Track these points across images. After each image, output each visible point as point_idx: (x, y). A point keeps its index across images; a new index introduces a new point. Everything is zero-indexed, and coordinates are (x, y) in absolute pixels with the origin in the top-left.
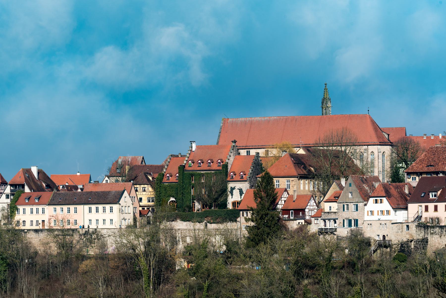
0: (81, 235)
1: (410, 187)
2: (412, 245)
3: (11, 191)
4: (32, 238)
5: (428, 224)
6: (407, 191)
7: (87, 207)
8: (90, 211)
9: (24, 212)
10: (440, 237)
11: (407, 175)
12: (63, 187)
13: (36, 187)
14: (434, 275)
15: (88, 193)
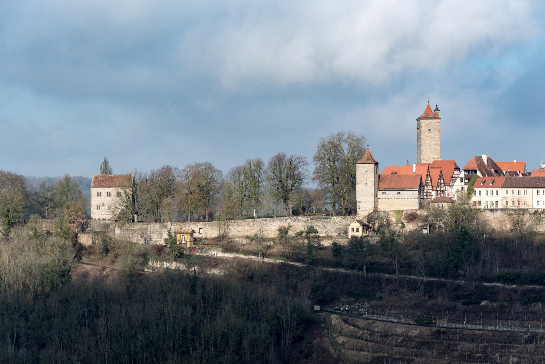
0: (531, 214)
3: (465, 175)
4: (488, 217)
7: (535, 190)
8: (538, 193)
9: (480, 194)
12: (506, 172)
13: (487, 173)
15: (536, 178)
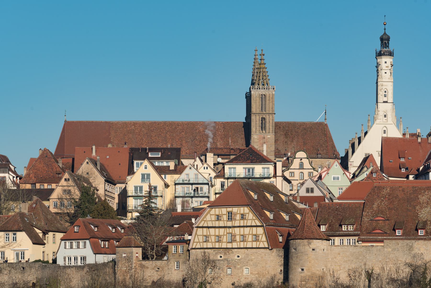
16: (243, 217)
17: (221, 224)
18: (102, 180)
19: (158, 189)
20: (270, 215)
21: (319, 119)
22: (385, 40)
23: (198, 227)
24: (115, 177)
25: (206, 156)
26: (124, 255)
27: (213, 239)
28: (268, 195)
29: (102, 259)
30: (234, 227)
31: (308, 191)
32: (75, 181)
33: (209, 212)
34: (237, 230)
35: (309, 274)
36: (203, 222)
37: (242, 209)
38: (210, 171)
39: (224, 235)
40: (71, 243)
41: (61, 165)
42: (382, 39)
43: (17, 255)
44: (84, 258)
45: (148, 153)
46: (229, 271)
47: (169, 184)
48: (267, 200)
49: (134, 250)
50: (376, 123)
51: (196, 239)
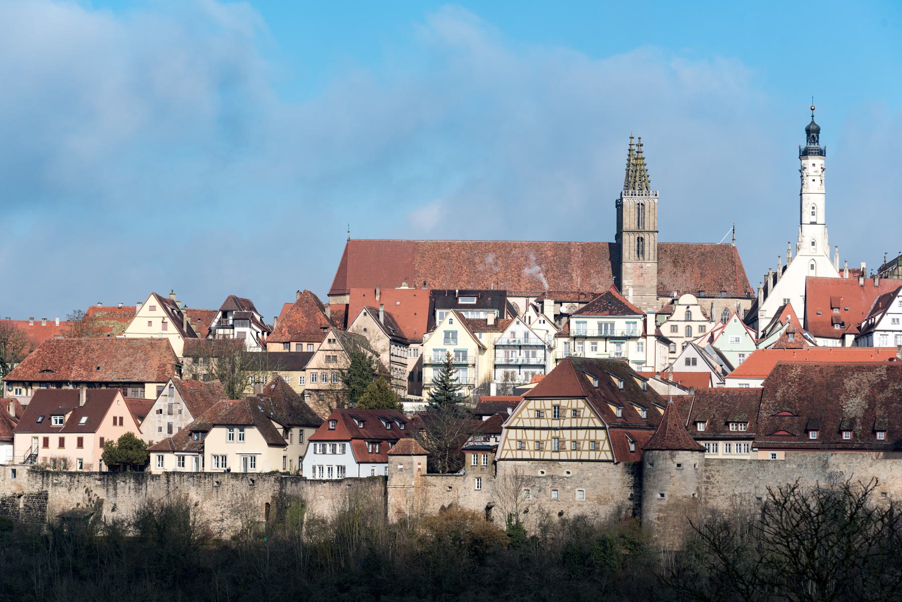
1: (18, 406)
2: (21, 503)
5: (48, 469)
6: (12, 413)
10: (69, 490)
11: (8, 384)
14: (61, 554)
16: (576, 413)
17: (544, 423)
18: (386, 340)
19: (469, 354)
20: (617, 412)
21: (724, 239)
22: (812, 133)
23: (509, 428)
24: (408, 335)
25: (542, 303)
26: (400, 467)
27: (531, 445)
28: (615, 380)
29: (366, 471)
30: (563, 429)
31: (688, 362)
32: (343, 342)
33: (525, 406)
34: (567, 433)
35: (672, 501)
36: (517, 420)
37: (574, 401)
38: (548, 326)
39: (548, 440)
40: (323, 445)
41: (328, 315)
42: (808, 131)
43: (245, 460)
44: (342, 469)
45: (457, 299)
46: (554, 495)
47: (486, 345)
48: (613, 387)
49: (416, 459)
50: (799, 253)
51: (506, 443)
